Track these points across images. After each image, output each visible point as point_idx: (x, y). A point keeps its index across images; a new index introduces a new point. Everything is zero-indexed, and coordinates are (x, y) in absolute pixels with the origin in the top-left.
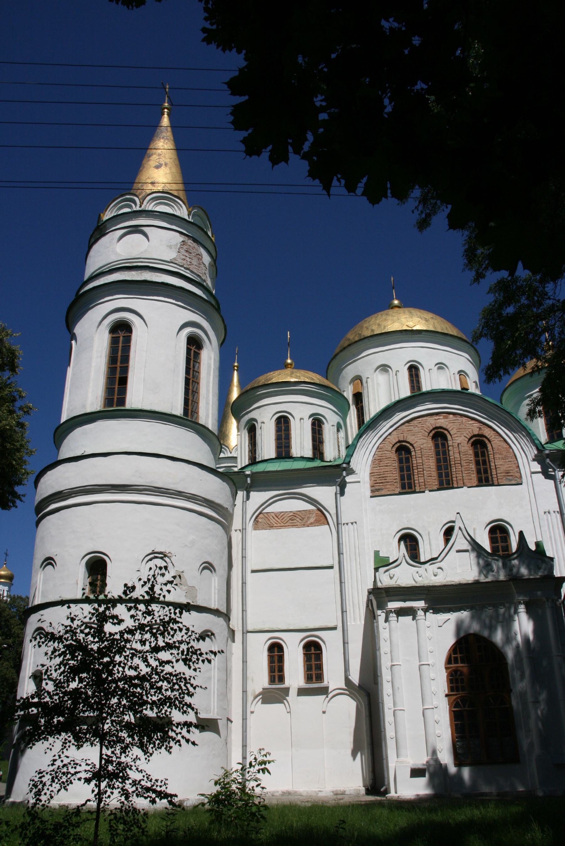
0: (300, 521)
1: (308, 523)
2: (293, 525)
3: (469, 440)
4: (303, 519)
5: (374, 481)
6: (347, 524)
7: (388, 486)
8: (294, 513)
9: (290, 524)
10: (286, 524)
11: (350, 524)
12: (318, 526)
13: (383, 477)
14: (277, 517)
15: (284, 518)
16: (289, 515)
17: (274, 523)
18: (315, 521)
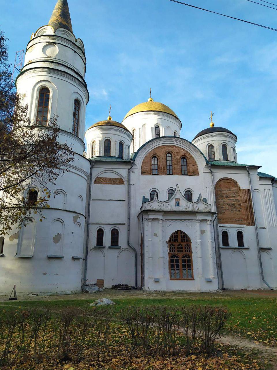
1: (117, 183)
3: (181, 157)
4: (114, 181)
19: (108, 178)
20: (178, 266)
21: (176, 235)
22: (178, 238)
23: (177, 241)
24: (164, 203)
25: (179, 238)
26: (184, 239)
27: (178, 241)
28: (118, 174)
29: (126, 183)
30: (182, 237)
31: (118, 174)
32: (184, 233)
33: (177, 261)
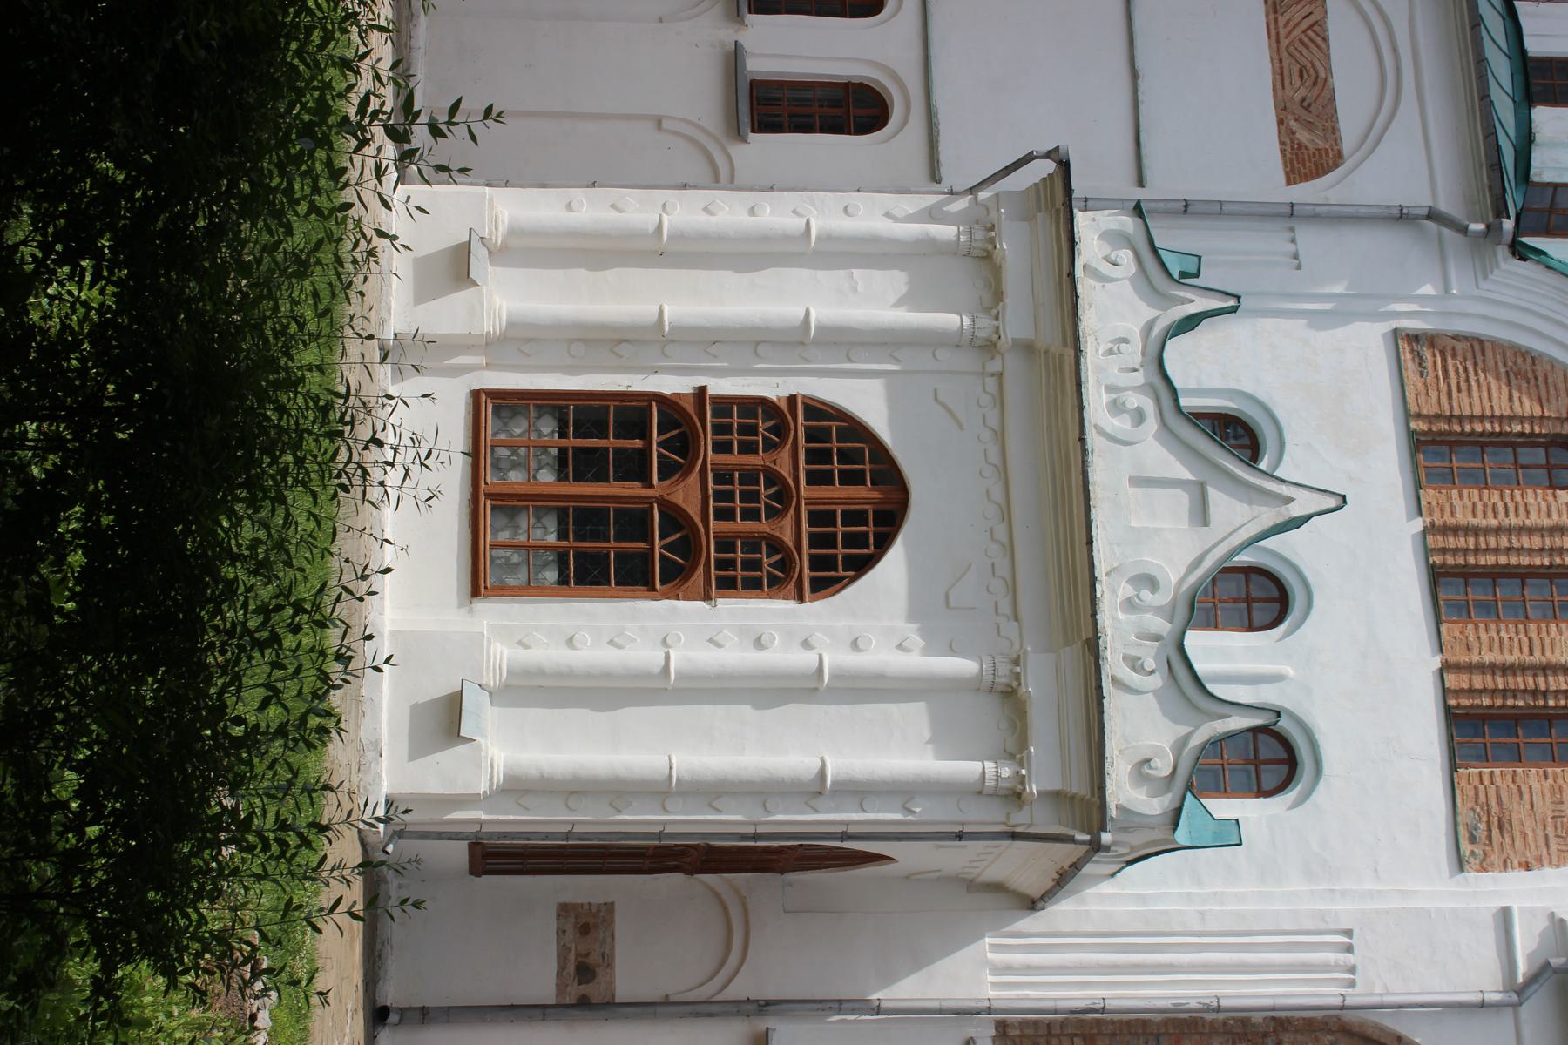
0: (1297, 97)
1: (1294, 125)
2: (1282, 74)
4: (1307, 109)
5: (1454, 349)
6: (1293, 241)
7: (1434, 395)
8: (1326, 80)
9: (1285, 64)
10: (1284, 55)
11: (1291, 248)
12: (1283, 151)
13: (1467, 380)
14: (1310, 27)
15: (1307, 47)
16: (1317, 63)
17: (1287, 16)
18: (1300, 146)
19: (1328, 57)
20: (586, 465)
23: (814, 480)
27: (808, 483)
29: (1305, 192)
33: (635, 467)
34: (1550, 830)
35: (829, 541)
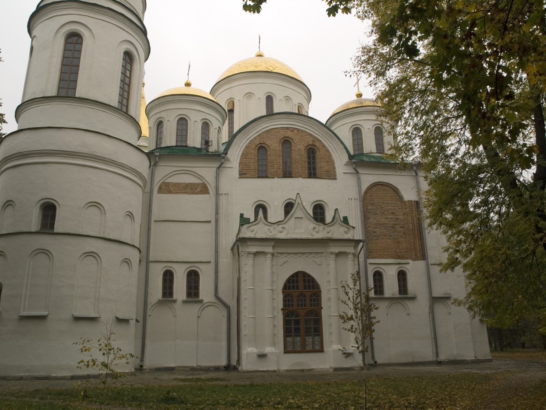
0: (190, 190)
1: (196, 191)
3: (306, 147)
4: (193, 188)
5: (242, 168)
6: (222, 194)
7: (251, 172)
8: (186, 184)
10: (180, 192)
11: (224, 195)
12: (202, 194)
15: (179, 187)
17: (172, 190)
19: (181, 183)
20: (297, 330)
21: (295, 278)
22: (298, 283)
23: (298, 288)
24: (275, 226)
25: (301, 284)
26: (290, 283)
27: (299, 289)
28: (200, 177)
29: (212, 190)
30: (305, 280)
31: (200, 177)
32: (309, 276)
33: (297, 322)
34: (328, 164)
35: (309, 286)
